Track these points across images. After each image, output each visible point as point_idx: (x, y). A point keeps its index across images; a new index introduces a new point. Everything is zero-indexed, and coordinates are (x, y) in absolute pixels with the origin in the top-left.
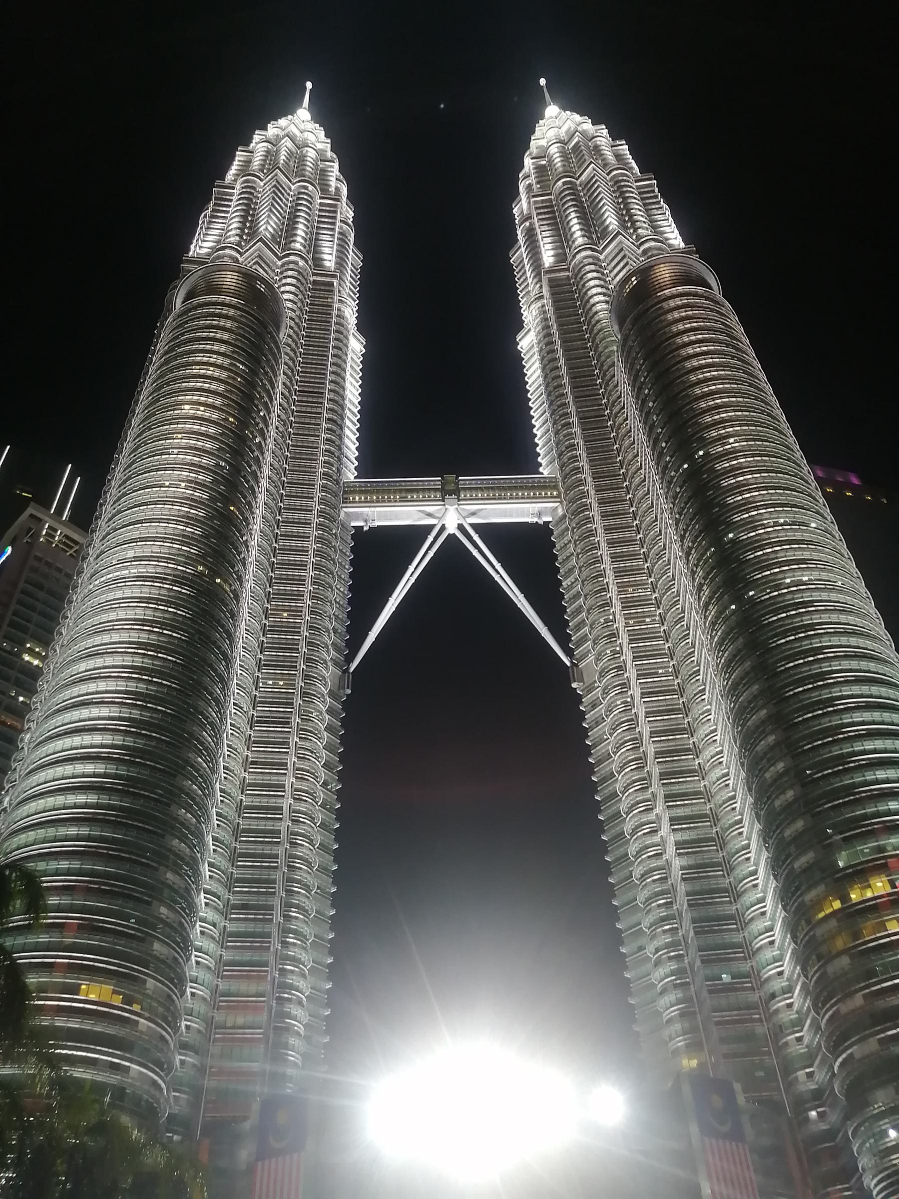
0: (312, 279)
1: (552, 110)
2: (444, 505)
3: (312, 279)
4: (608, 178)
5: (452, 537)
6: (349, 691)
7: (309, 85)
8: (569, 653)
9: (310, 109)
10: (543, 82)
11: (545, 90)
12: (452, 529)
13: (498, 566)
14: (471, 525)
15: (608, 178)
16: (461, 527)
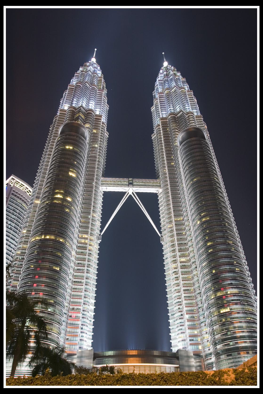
0: (95, 117)
1: (166, 64)
2: (129, 187)
3: (95, 117)
4: (180, 91)
5: (130, 195)
6: (101, 241)
7: (96, 49)
8: (161, 233)
9: (96, 57)
10: (163, 53)
11: (164, 56)
12: (130, 193)
13: (143, 206)
14: (136, 193)
15: (180, 91)
16: (133, 193)
